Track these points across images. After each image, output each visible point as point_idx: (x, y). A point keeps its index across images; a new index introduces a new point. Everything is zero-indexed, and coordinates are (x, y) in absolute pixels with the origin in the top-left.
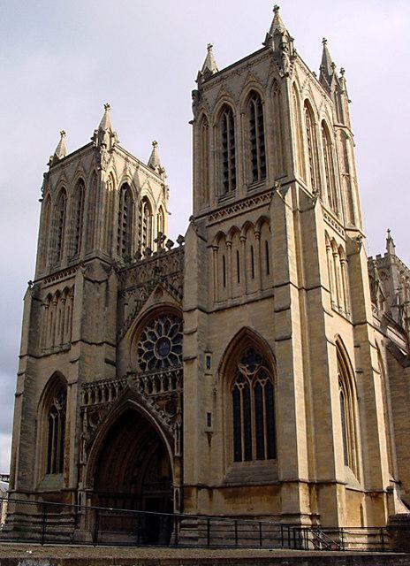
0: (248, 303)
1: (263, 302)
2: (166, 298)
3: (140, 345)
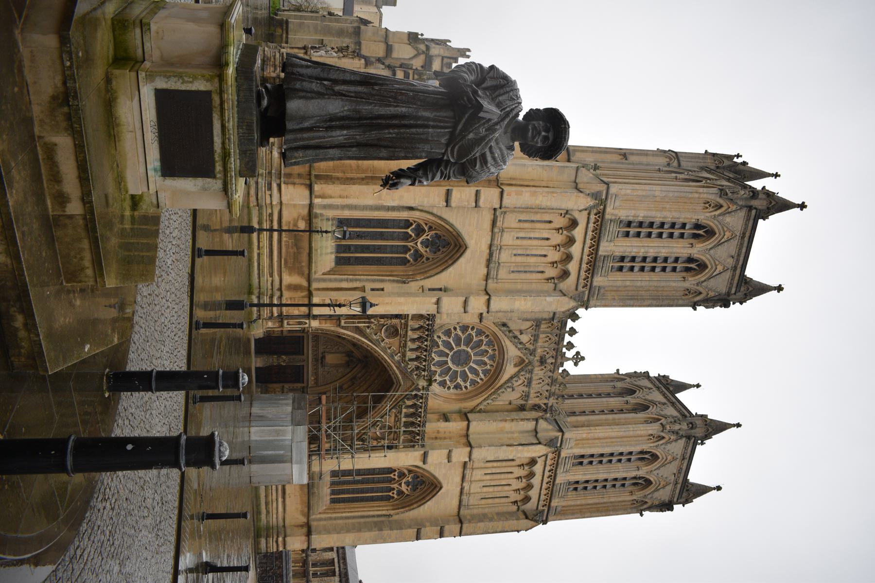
0: (462, 489)
2: (510, 370)
3: (473, 328)
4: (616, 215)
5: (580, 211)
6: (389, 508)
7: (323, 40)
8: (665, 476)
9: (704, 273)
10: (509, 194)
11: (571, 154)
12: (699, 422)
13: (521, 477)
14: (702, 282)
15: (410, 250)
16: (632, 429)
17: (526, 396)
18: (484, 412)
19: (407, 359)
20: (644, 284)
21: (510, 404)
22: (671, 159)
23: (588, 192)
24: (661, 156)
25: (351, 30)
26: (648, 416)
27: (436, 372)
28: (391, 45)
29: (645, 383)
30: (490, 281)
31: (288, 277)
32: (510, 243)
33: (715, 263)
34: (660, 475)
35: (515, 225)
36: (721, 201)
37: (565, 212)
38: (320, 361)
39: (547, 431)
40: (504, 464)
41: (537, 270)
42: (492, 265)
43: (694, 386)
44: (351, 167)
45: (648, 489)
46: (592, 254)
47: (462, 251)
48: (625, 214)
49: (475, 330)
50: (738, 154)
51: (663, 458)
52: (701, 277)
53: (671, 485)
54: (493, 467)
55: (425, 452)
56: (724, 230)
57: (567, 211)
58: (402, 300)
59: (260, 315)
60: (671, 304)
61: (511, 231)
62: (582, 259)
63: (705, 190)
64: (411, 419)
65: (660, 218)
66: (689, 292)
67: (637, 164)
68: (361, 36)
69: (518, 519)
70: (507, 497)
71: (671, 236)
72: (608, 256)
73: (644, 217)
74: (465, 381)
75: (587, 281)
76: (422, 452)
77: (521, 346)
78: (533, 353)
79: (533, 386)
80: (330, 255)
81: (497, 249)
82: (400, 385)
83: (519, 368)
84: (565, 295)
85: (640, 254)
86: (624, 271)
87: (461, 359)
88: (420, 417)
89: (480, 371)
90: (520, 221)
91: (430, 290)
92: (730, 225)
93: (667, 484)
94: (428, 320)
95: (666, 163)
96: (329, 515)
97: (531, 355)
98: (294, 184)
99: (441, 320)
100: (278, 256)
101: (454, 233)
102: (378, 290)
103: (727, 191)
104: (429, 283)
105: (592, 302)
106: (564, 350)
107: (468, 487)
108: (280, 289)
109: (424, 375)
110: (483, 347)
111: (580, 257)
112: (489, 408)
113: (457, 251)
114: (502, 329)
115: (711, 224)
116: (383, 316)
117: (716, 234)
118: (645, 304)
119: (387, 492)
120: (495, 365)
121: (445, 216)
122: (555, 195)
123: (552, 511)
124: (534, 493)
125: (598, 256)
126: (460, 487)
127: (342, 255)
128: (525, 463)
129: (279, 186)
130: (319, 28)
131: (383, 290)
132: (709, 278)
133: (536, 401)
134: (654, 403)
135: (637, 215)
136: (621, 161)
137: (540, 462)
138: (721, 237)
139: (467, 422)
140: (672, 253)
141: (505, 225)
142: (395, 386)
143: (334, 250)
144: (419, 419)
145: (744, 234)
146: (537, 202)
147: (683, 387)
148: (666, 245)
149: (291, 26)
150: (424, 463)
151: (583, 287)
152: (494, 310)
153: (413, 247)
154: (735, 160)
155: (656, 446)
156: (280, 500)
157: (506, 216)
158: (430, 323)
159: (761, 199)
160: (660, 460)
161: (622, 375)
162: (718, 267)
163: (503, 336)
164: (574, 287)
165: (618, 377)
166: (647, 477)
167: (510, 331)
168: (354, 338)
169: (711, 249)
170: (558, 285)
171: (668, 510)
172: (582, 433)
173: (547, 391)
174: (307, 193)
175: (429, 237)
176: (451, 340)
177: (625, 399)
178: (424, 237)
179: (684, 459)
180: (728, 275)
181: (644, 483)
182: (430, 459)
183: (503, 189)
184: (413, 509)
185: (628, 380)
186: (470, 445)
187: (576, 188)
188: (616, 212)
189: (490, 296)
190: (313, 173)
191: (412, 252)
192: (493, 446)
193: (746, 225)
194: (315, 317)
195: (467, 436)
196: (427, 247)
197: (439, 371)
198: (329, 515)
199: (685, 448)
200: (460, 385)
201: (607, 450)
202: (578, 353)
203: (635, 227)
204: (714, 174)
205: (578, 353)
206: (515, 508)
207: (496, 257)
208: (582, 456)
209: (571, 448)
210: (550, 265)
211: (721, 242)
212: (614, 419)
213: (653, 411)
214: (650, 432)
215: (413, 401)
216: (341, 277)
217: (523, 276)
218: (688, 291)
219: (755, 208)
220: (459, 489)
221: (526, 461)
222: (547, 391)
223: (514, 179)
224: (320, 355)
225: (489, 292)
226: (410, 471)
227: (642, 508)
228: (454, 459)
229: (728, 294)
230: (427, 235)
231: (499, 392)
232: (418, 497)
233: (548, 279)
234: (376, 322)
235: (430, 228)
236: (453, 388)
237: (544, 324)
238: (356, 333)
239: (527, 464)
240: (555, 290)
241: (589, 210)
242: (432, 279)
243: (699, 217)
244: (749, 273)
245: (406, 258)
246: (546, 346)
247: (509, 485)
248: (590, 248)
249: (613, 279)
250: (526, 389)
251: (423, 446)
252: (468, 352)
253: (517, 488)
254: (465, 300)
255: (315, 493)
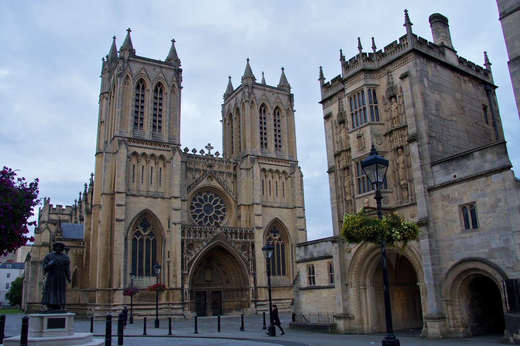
1: (284, 209)
2: (214, 183)
3: (192, 203)
4: (131, 131)
5: (128, 151)
6: (288, 245)
7: (39, 283)
8: (274, 99)
9: (163, 83)
10: (118, 189)
11: (101, 151)
12: (245, 82)
13: (272, 176)
14: (168, 84)
15: (148, 238)
16: (247, 118)
17: (229, 174)
18: (237, 196)
19: (205, 239)
20: (168, 115)
21: (233, 183)
22: (104, 97)
23: (118, 147)
24: (102, 102)
25: (34, 267)
26: (241, 108)
27: (215, 222)
28: (42, 243)
29: (227, 106)
30: (165, 197)
31: (162, 300)
32: (145, 186)
33: (158, 78)
34: (273, 102)
35: (135, 184)
36: (125, 76)
37: (129, 158)
38: (209, 283)
39: (246, 163)
40: (265, 185)
41: (159, 172)
42: (156, 196)
43: (230, 80)
44: (105, 269)
45: (281, 108)
46: (151, 143)
47: (149, 212)
48: (129, 127)
49: (193, 202)
50: (102, 59)
51: (264, 101)
52: (165, 84)
53: (279, 95)
54: (266, 191)
55: (256, 228)
56: (140, 74)
57: (128, 157)
58: (173, 242)
59: (182, 314)
60: (179, 100)
61: (139, 186)
62: (154, 149)
63: (118, 85)
64: (238, 235)
65: (132, 108)
66: (173, 90)
67: (106, 116)
68: (36, 261)
69: (294, 177)
70: (283, 183)
71: (143, 101)
72: (152, 135)
73: (132, 117)
74: (221, 207)
75: (166, 145)
76: (256, 229)
77: (201, 178)
78: (205, 171)
79: (223, 171)
80: (151, 279)
81: (148, 193)
82: (220, 242)
83: (213, 178)
84: (172, 158)
85: (152, 117)
86: (161, 126)
87: (209, 208)
88: (237, 231)
89: (215, 199)
90: (133, 182)
91: (169, 228)
92: (138, 70)
93: (278, 97)
94: (185, 228)
95: (106, 100)
96: (291, 276)
97: (206, 173)
98: (113, 298)
99: (185, 221)
100: (151, 306)
101: (139, 216)
102: (169, 254)
103: (119, 73)
104: (166, 228)
105: (177, 142)
106: (204, 155)
107: (277, 204)
108: (169, 304)
109: (215, 229)
110: (202, 198)
111: (153, 150)
112: (235, 193)
113: (149, 214)
114: (192, 188)
115: (137, 80)
116: (182, 252)
117: (142, 78)
118: (179, 114)
119: (279, 246)
120: (212, 191)
121: (130, 221)
122: (119, 165)
123: (291, 159)
124: (281, 169)
125: (153, 140)
126: (277, 208)
127: (151, 273)
128: (264, 175)
129: (114, 306)
130: (32, 285)
131: (169, 252)
132: (166, 81)
133: (232, 168)
134: (236, 104)
135: (131, 120)
136: (104, 124)
137: (263, 166)
138: (144, 75)
139: (241, 206)
140: (152, 101)
141: (135, 189)
142: (220, 244)
143: (149, 277)
144: (238, 231)
145: (142, 63)
146: (123, 174)
147: (230, 86)
148: (147, 105)
149: (31, 301)
150: (261, 228)
151: (169, 147)
152: (180, 195)
153: (147, 237)
154: (106, 60)
155: (257, 105)
156: (282, 301)
157: (131, 189)
158: (186, 227)
159: (124, 54)
160: (265, 102)
161: (223, 119)
162: (160, 76)
163: (196, 187)
164: (169, 152)
165: (224, 121)
166: (274, 108)
167: (193, 184)
168: (194, 266)
169: (150, 80)
170: (168, 161)
171: (293, 96)
172: (248, 144)
173: (226, 163)
174: (118, 291)
175: (142, 229)
176: (198, 215)
177: (234, 119)
178: (142, 231)
179: (265, 90)
180: (164, 70)
181: (278, 110)
182: (260, 226)
183: (116, 192)
184: (288, 232)
185: (225, 116)
186: (253, 204)
187: (116, 153)
188: (129, 131)
189: (172, 197)
190: (108, 289)
191: (149, 237)
192: (253, 192)
193: (138, 62)
194: (183, 286)
195: (249, 205)
196: (147, 230)
197: (215, 221)
198: (291, 276)
199: (259, 89)
200: (223, 209)
201: (258, 131)
202: (206, 147)
203: (138, 121)
204: (112, 75)
205: (206, 147)
206: (289, 179)
207: (152, 194)
208: (262, 143)
209: (256, 150)
210: (157, 165)
211: (146, 75)
212: (243, 127)
213: (240, 106)
214: (249, 108)
215: (228, 235)
216: (162, 273)
217: (162, 179)
218: (173, 91)
219: (129, 57)
220: (278, 209)
221: (263, 174)
222: (226, 163)
223: (111, 185)
224: (207, 283)
225: (170, 197)
226: (268, 235)
227: (291, 111)
228: (260, 212)
229: (175, 70)
230: (141, 229)
231: (226, 189)
232: (282, 229)
233: (164, 166)
234: (186, 255)
235: (137, 228)
236: (225, 213)
237: (190, 166)
238: (192, 265)
239: (265, 173)
240: (170, 162)
241: (127, 146)
242: (163, 227)
243: (133, 87)
244: (163, 60)
245: (153, 240)
246: (202, 164)
247: (276, 182)
248: (148, 144)
249: (165, 132)
250: (225, 175)
251: (253, 229)
252: (205, 206)
253: (278, 178)
254: (174, 210)
255: (279, 284)
